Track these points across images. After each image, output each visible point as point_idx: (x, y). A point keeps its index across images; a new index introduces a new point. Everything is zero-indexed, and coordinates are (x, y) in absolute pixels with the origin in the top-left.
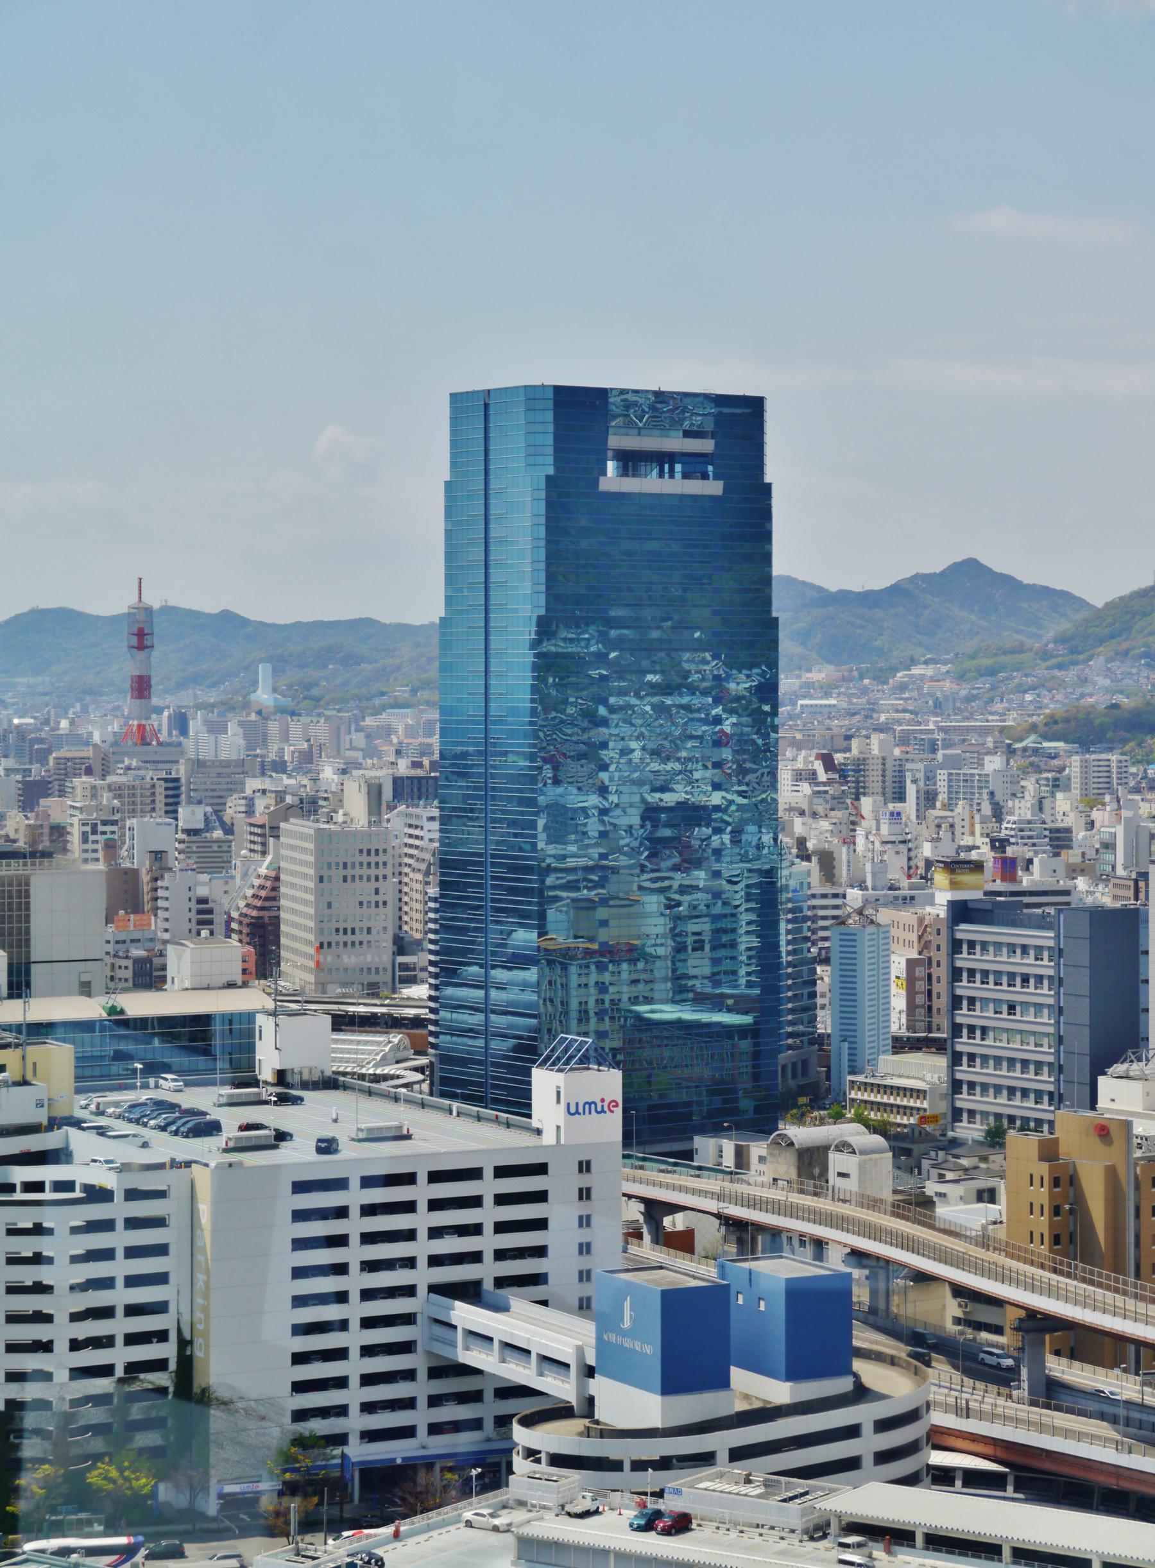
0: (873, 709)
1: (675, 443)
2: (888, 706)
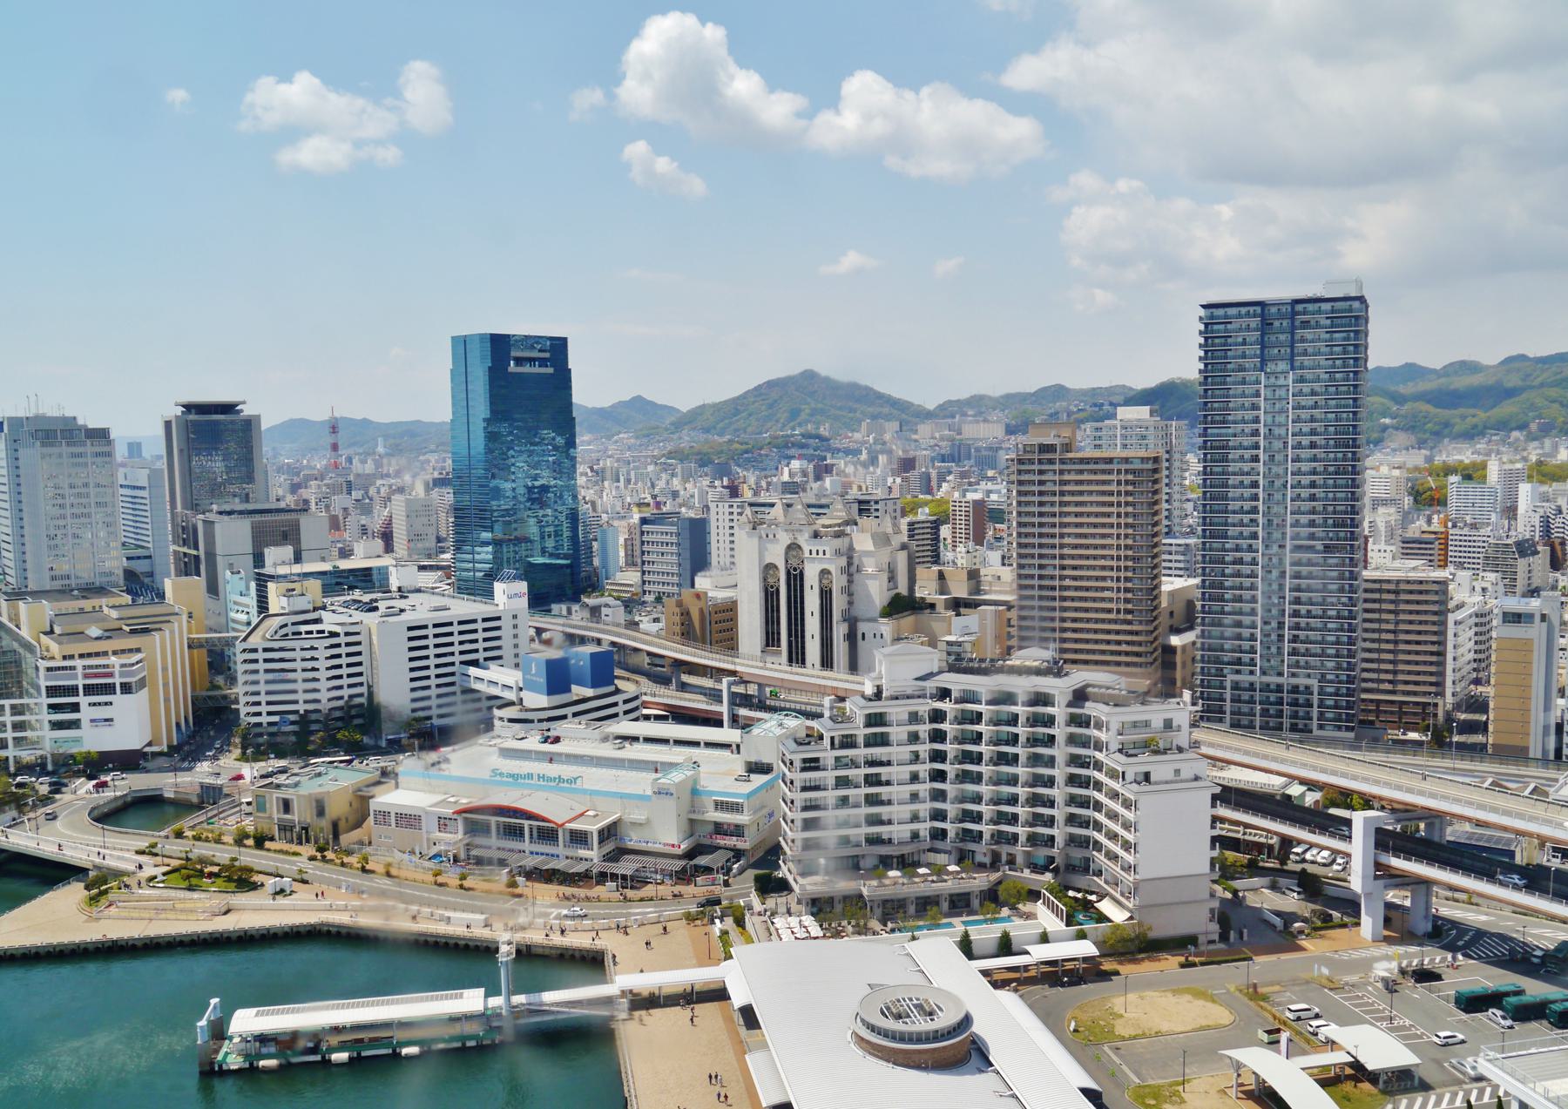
0: (606, 450)
1: (535, 354)
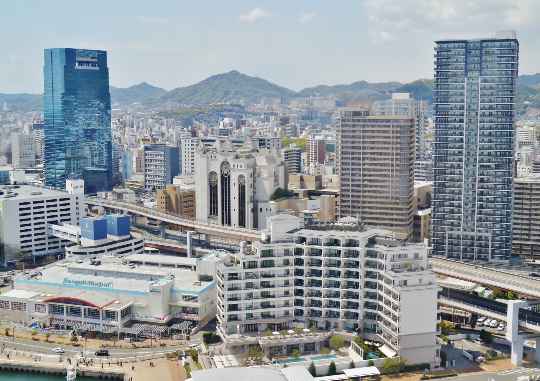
1: (89, 59)
2: (130, 110)
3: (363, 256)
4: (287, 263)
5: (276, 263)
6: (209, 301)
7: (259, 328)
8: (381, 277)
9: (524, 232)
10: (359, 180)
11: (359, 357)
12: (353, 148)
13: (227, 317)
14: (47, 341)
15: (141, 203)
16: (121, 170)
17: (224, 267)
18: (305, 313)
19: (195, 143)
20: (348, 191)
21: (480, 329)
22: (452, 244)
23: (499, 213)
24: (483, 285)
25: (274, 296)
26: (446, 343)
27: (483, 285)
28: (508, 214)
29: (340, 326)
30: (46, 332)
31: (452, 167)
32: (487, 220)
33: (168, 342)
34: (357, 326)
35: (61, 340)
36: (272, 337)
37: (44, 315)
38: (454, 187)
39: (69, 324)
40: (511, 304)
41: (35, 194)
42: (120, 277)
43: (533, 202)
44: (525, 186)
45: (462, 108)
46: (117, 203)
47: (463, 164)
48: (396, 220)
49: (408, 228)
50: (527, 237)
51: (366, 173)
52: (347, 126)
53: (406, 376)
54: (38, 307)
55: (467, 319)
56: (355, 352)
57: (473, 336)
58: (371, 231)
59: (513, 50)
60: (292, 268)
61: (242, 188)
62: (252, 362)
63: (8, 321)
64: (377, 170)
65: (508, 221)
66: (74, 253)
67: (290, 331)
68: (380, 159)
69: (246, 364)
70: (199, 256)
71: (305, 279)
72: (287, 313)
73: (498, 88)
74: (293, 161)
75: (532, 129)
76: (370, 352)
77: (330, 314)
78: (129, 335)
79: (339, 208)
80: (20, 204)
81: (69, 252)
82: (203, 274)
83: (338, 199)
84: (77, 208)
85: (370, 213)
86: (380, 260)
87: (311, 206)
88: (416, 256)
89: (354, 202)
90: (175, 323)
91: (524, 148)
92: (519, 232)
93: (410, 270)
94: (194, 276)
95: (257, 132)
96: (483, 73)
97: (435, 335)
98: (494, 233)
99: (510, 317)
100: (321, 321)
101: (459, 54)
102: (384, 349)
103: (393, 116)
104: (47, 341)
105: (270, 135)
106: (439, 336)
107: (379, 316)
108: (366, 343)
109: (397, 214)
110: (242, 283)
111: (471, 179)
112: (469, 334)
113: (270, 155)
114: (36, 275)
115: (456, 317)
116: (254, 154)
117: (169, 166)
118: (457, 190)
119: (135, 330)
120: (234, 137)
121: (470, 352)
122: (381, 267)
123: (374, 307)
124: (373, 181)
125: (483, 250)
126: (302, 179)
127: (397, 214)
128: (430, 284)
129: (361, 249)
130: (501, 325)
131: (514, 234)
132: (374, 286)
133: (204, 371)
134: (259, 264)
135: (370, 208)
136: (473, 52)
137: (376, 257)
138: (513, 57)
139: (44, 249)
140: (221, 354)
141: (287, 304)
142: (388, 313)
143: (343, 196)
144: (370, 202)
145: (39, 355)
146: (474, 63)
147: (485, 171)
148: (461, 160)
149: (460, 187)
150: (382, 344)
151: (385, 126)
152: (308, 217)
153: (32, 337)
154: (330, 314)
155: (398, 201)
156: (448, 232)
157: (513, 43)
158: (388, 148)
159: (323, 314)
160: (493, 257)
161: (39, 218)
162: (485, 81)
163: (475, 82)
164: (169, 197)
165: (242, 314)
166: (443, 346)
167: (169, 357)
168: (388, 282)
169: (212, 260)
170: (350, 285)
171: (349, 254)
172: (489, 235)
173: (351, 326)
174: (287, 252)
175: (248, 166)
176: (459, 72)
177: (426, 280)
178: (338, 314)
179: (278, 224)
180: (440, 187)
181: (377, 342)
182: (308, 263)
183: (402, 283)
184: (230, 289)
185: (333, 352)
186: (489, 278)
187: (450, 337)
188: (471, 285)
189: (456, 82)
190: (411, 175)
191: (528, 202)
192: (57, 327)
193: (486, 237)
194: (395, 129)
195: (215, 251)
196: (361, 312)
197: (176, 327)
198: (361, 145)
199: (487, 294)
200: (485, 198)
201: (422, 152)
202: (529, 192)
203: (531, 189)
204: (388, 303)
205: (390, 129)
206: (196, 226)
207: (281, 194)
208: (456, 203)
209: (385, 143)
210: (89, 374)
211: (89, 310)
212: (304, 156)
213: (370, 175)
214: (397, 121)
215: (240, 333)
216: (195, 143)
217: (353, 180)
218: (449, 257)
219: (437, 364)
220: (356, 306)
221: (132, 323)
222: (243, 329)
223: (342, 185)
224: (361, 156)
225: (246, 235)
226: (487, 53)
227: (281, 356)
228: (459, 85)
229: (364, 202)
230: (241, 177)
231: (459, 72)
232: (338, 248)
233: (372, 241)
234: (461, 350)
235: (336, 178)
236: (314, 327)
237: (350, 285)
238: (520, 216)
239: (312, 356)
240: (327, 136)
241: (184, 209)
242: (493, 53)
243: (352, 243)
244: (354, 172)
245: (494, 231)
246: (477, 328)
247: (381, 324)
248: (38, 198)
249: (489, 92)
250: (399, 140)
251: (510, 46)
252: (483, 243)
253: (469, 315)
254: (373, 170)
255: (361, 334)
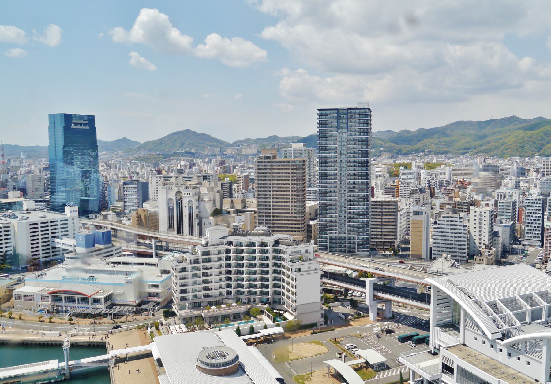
3: (271, 252)
4: (220, 259)
5: (212, 259)
6: (167, 288)
7: (202, 305)
8: (283, 267)
9: (378, 233)
10: (270, 202)
11: (270, 321)
12: (265, 180)
13: (179, 298)
14: (50, 322)
15: (120, 221)
16: (107, 198)
17: (176, 263)
18: (233, 293)
19: (158, 179)
20: (263, 209)
21: (350, 298)
22: (332, 243)
23: (361, 221)
24: (352, 269)
25: (211, 282)
26: (327, 309)
27: (352, 269)
28: (367, 222)
29: (257, 300)
30: (49, 315)
31: (331, 192)
32: (354, 226)
33: (138, 317)
34: (268, 300)
35: (60, 321)
36: (211, 310)
37: (48, 303)
38: (332, 205)
39: (67, 309)
40: (368, 281)
41: (42, 217)
42: (104, 273)
43: (384, 213)
44: (378, 203)
45: (336, 153)
46: (103, 222)
47: (337, 190)
48: (295, 228)
49: (303, 233)
50: (380, 237)
51: (274, 197)
52: (261, 165)
53: (302, 332)
54: (43, 298)
55: (342, 292)
56: (267, 318)
57: (345, 303)
58: (277, 236)
59: (367, 115)
60: (224, 263)
61: (190, 209)
62: (197, 328)
63: (21, 309)
64: (281, 195)
65: (367, 226)
66: (71, 258)
67: (223, 306)
68: (283, 187)
69: (193, 330)
70: (160, 257)
71: (233, 269)
72: (221, 294)
73: (358, 139)
74: (227, 191)
75: (384, 166)
76: (277, 317)
77: (250, 293)
78: (110, 314)
79: (257, 221)
80: (31, 225)
81: (67, 258)
82: (163, 269)
83: (257, 215)
84: (73, 226)
85: (278, 224)
86: (282, 255)
87: (238, 221)
88: (306, 251)
89: (267, 216)
90: (144, 304)
91: (379, 178)
92: (375, 233)
93: (303, 261)
94: (156, 271)
95: (203, 171)
96: (349, 130)
97: (320, 304)
98: (358, 235)
99: (368, 290)
100: (244, 298)
101: (333, 118)
102: (287, 315)
103: (293, 159)
104: (50, 322)
105: (212, 172)
106: (323, 304)
107: (283, 293)
108: (275, 311)
109: (295, 224)
110: (189, 274)
111: (343, 200)
112: (342, 302)
113: (210, 186)
114: (42, 275)
115: (334, 291)
116: (198, 186)
117: (141, 195)
118: (334, 207)
119: (115, 310)
120: (185, 175)
121: (343, 314)
122: (283, 260)
123: (279, 287)
124: (279, 202)
125: (352, 246)
126: (232, 202)
127: (295, 224)
128: (316, 269)
129: (270, 248)
130: (364, 295)
131: (372, 235)
132: (279, 272)
133: (163, 336)
134: (201, 261)
135: (278, 220)
136: (342, 116)
137: (280, 253)
138: (367, 120)
139: (49, 256)
140: (176, 324)
141: (221, 287)
142: (288, 291)
143: (259, 213)
144: (277, 217)
145: (44, 332)
146: (343, 123)
147: (352, 194)
148: (336, 187)
149: (336, 205)
150: (285, 312)
151: (286, 165)
152: (236, 227)
153: (38, 319)
154: (250, 293)
155: (296, 215)
156: (329, 235)
157: (367, 110)
158: (288, 180)
159: (246, 293)
160: (358, 251)
161: (45, 234)
162: (350, 135)
163: (344, 136)
164: (140, 217)
165: (190, 295)
166: (325, 310)
167: (139, 328)
168: (288, 269)
169: (169, 259)
170: (263, 272)
171: (262, 252)
172: (356, 236)
173: (265, 301)
174: (220, 252)
175: (195, 194)
176: (333, 129)
177: (313, 268)
178: (256, 292)
179: (215, 233)
180: (323, 204)
181: (282, 310)
182: (234, 259)
183: (297, 270)
184: (181, 279)
185: (252, 319)
186: (354, 265)
187: (330, 305)
188: (344, 269)
189: (332, 136)
190: (304, 198)
191: (380, 213)
192: (58, 312)
193: (354, 238)
194: (293, 167)
195: (171, 253)
196: (270, 290)
197: (144, 307)
198: (271, 178)
199: (354, 275)
200: (352, 211)
201: (312, 182)
202: (380, 207)
203: (382, 205)
204: (288, 284)
205: (290, 167)
206: (158, 236)
207: (217, 213)
208: (334, 216)
209: (287, 177)
210: (81, 344)
211: (81, 298)
212: (235, 186)
213: (277, 198)
214: (294, 162)
215: (189, 308)
216: (158, 179)
217: (266, 202)
218: (330, 251)
219: (321, 323)
220: (268, 286)
221: (113, 305)
222: (191, 306)
223: (259, 205)
224: (271, 186)
225: (193, 241)
226: (351, 117)
227: (218, 323)
228: (334, 138)
229: (273, 217)
230: (190, 201)
231: (333, 129)
232: (254, 248)
233: (277, 243)
234: (338, 313)
235: (255, 201)
236: (239, 302)
237: (263, 272)
238: (375, 223)
239: (238, 322)
240: (250, 173)
241: (151, 225)
242: (355, 117)
243: (264, 244)
244: (267, 197)
245: (359, 233)
246: (348, 298)
247: (284, 298)
248: (44, 220)
249: (353, 142)
250: (295, 175)
251: (365, 112)
252: (352, 241)
253: (343, 289)
254: (279, 195)
255: (271, 306)
